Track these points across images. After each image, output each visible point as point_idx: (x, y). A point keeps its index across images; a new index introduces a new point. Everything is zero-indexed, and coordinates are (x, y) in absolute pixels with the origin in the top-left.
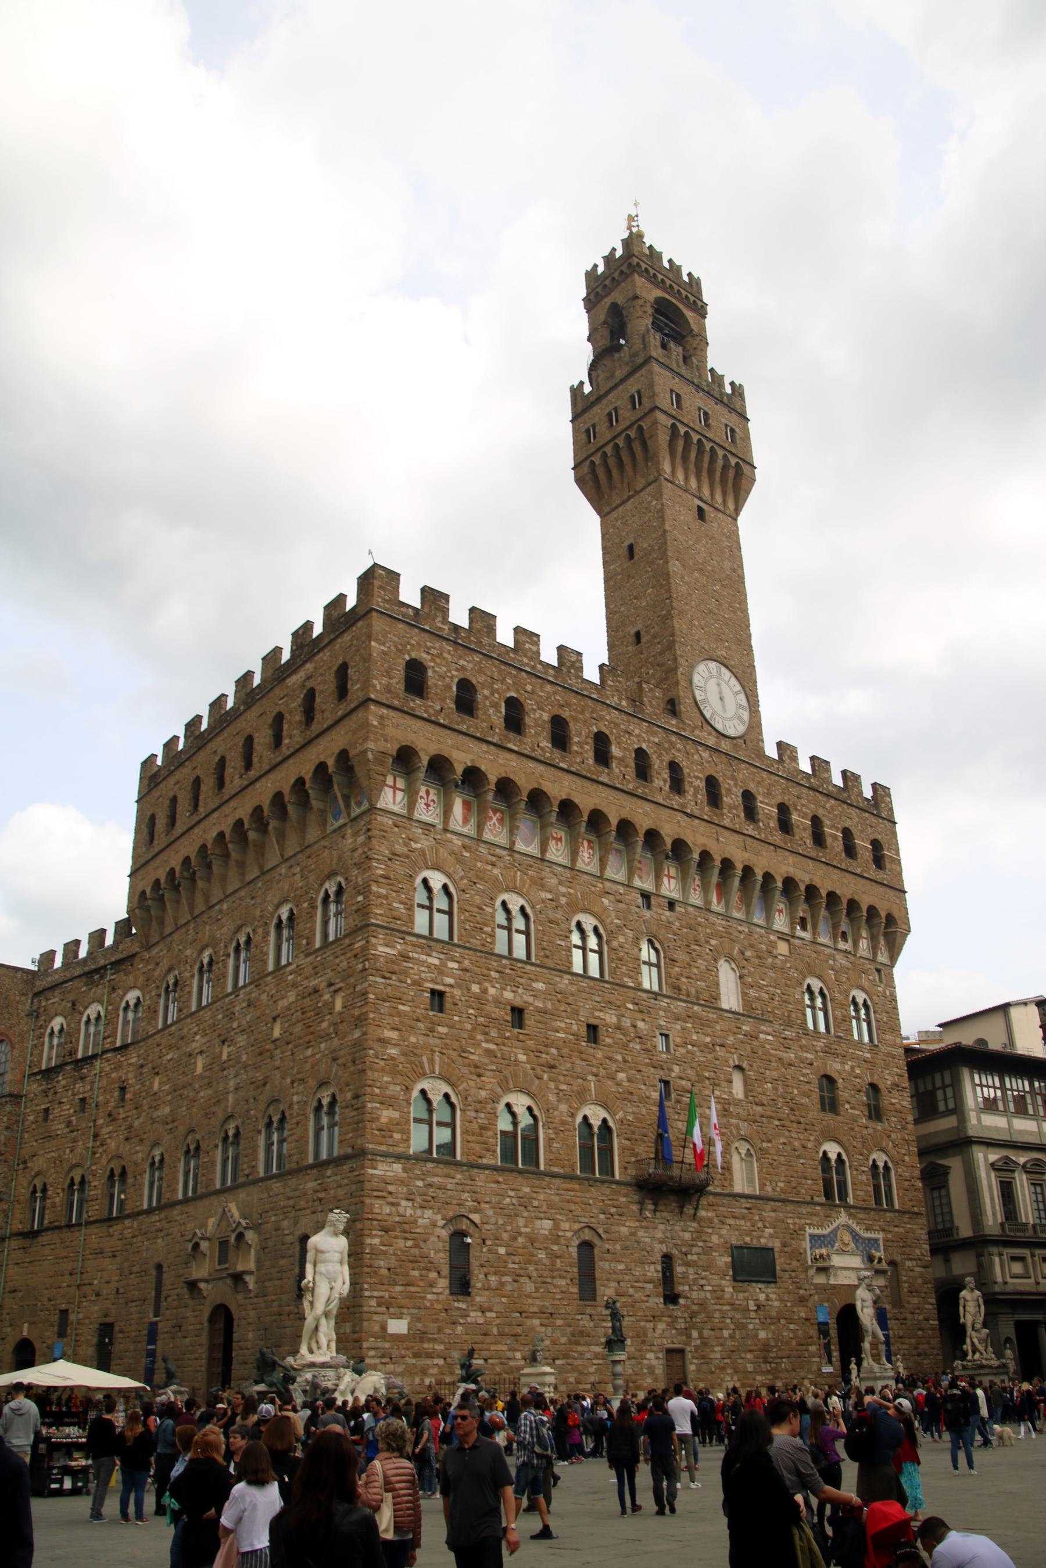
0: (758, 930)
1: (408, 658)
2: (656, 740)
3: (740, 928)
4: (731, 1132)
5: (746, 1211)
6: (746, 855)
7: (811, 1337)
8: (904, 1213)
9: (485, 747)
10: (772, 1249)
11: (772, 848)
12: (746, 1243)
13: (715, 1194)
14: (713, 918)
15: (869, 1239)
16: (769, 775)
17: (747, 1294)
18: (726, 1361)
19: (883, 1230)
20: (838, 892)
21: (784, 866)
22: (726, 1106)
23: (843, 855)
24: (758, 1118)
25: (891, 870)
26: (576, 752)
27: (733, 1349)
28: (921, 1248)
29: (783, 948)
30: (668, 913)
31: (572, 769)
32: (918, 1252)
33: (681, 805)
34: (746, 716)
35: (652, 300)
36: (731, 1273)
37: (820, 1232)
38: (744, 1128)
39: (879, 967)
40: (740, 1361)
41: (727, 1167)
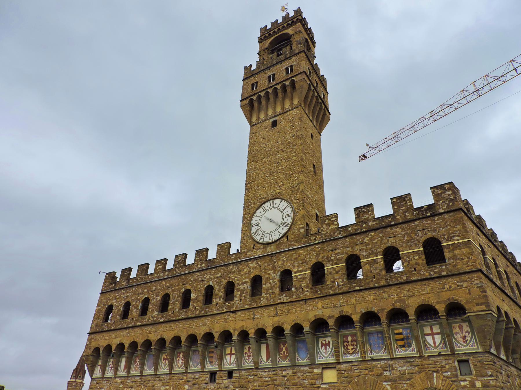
0: (302, 368)
1: (107, 306)
2: (219, 275)
3: (284, 373)
6: (276, 319)
9: (127, 331)
11: (301, 302)
14: (260, 373)
16: (306, 249)
20: (375, 309)
21: (305, 315)
23: (384, 273)
25: (454, 257)
26: (171, 309)
29: (330, 376)
30: (226, 381)
31: (166, 320)
33: (230, 307)
34: (289, 220)
35: (267, 46)
39: (464, 358)
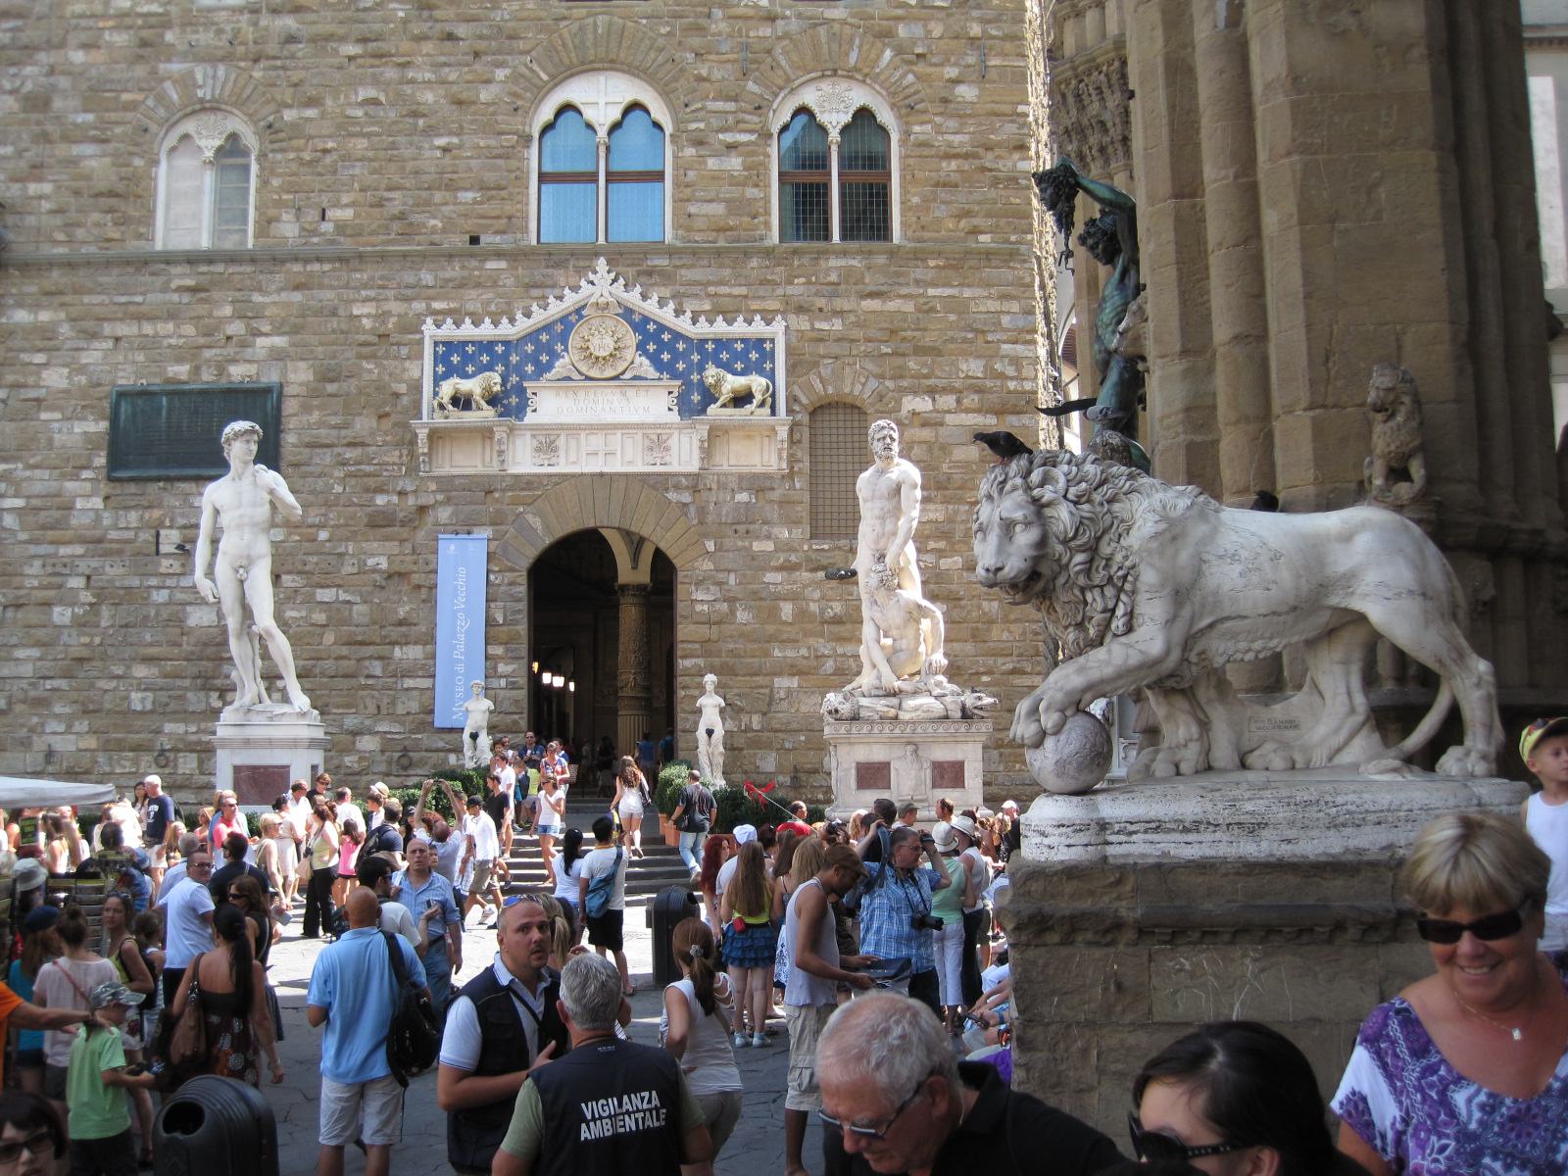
4: (161, 98)
5: (186, 298)
7: (401, 623)
8: (918, 256)
10: (267, 391)
12: (168, 381)
13: (70, 265)
15: (722, 343)
17: (156, 513)
18: (49, 684)
19: (801, 310)
22: (145, 33)
24: (272, 48)
27: (85, 653)
28: (990, 355)
32: (974, 367)
36: (101, 460)
37: (486, 331)
38: (209, 80)
40: (102, 684)
41: (130, 198)
